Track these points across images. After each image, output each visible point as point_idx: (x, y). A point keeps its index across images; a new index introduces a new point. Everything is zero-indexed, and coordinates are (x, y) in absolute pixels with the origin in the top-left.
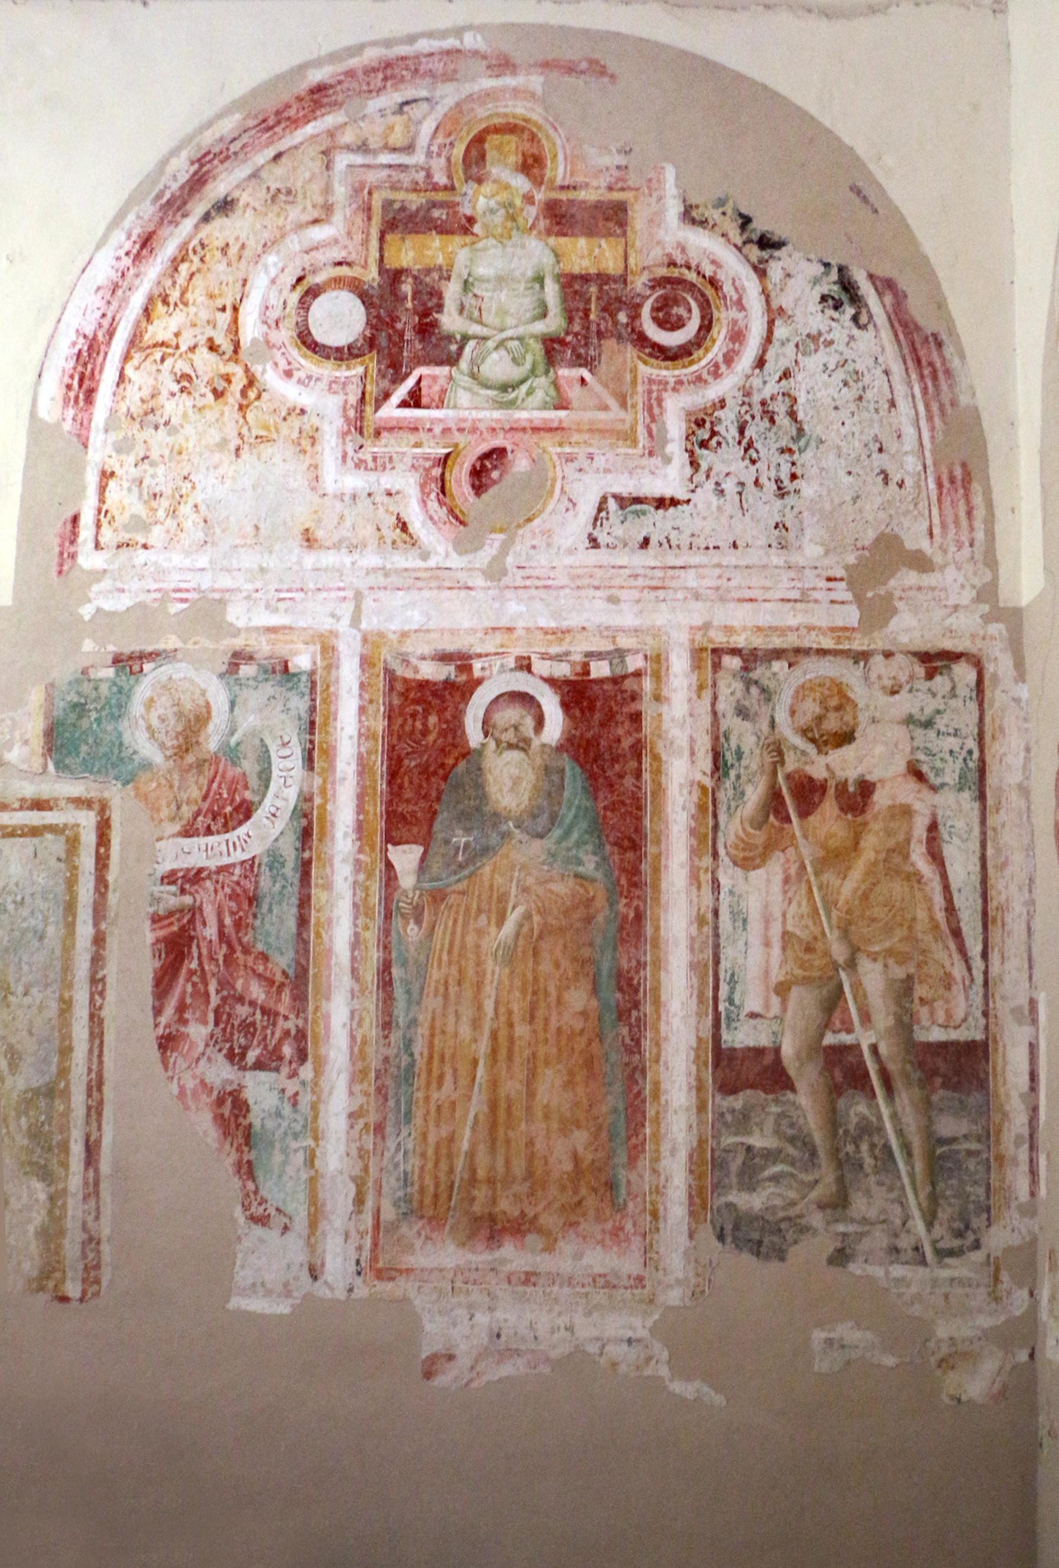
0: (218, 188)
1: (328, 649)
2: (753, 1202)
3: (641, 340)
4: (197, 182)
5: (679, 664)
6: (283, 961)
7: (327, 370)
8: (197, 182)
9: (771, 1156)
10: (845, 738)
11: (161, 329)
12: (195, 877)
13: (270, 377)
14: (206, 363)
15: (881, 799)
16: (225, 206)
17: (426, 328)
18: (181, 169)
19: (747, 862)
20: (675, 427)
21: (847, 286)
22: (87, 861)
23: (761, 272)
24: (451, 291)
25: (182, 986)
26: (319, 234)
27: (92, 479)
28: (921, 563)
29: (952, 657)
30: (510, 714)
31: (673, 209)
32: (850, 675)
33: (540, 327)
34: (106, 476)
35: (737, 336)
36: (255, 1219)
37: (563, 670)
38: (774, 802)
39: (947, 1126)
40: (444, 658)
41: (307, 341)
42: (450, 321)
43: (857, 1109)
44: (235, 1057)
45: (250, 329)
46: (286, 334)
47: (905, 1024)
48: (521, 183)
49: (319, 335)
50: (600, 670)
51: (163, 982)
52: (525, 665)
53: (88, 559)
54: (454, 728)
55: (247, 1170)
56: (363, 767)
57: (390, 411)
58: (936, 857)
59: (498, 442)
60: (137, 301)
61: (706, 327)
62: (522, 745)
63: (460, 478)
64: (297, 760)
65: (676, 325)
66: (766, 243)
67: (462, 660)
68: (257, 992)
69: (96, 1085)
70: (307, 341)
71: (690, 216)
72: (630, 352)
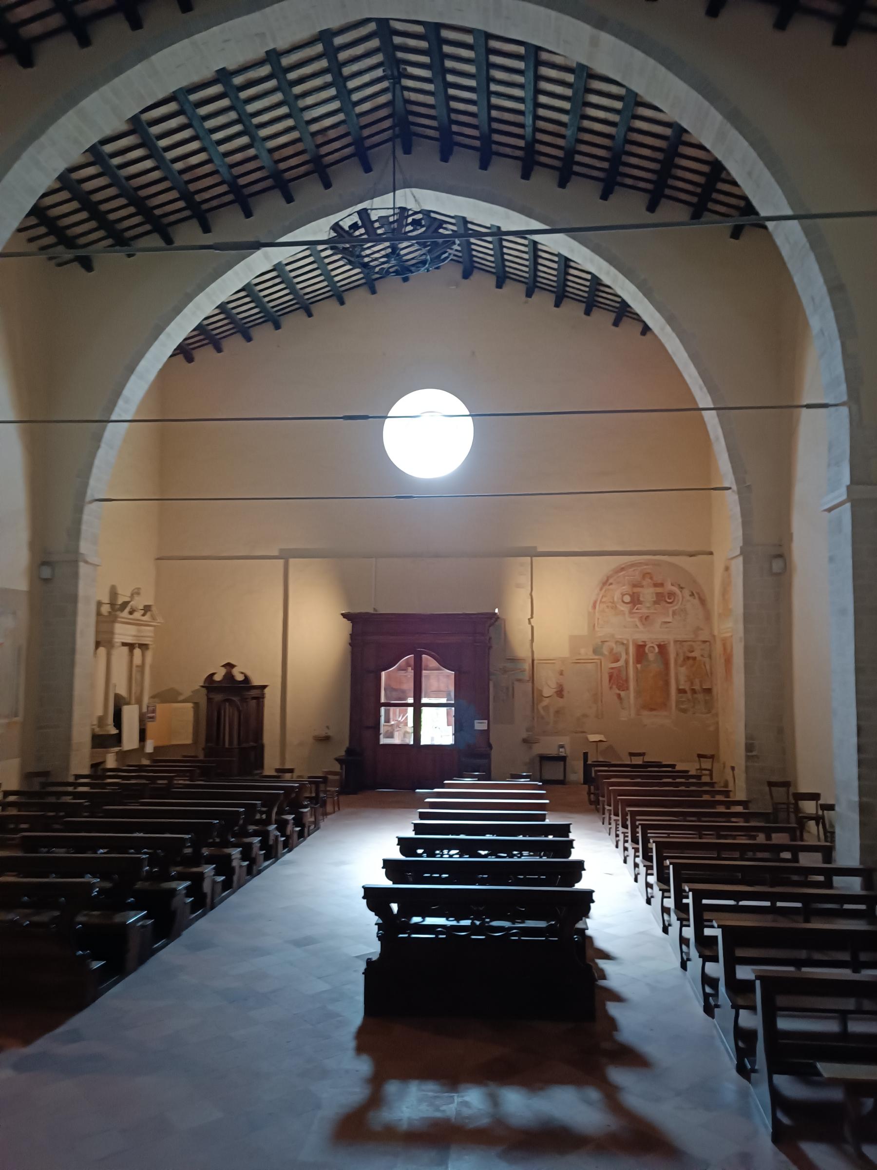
0: (611, 581)
1: (628, 640)
2: (683, 707)
3: (666, 601)
4: (607, 580)
5: (672, 643)
6: (624, 678)
7: (625, 605)
8: (607, 580)
9: (684, 701)
10: (693, 651)
11: (604, 600)
12: (612, 668)
13: (618, 606)
14: (610, 604)
15: (698, 659)
16: (611, 584)
17: (638, 600)
18: (605, 579)
19: (682, 666)
20: (671, 613)
21: (692, 593)
22: (599, 666)
23: (681, 591)
24: (641, 595)
25: (612, 681)
26: (624, 587)
27: (596, 619)
28: (702, 629)
29: (706, 641)
30: (652, 649)
31: (670, 584)
32: (693, 643)
33: (653, 600)
34: (598, 619)
35: (678, 600)
36: (623, 709)
37: (658, 643)
38: (684, 660)
39: (707, 698)
40: (643, 642)
41: (623, 602)
42: (641, 599)
43: (696, 696)
44: (619, 689)
45: (616, 599)
46: (620, 601)
47: (701, 686)
48: (650, 581)
49: (626, 601)
50: (662, 643)
51: (610, 681)
52: (652, 643)
53: (597, 629)
54: (644, 651)
55: (621, 703)
56: (633, 655)
57: (635, 611)
58: (705, 666)
59: (647, 615)
60: (601, 596)
61: (674, 599)
62: (652, 652)
63: (644, 620)
64: (625, 654)
65: (670, 599)
66: (682, 588)
67: (644, 642)
68: (621, 682)
69: (602, 693)
70: (623, 602)
71: (672, 585)
72: (665, 603)
